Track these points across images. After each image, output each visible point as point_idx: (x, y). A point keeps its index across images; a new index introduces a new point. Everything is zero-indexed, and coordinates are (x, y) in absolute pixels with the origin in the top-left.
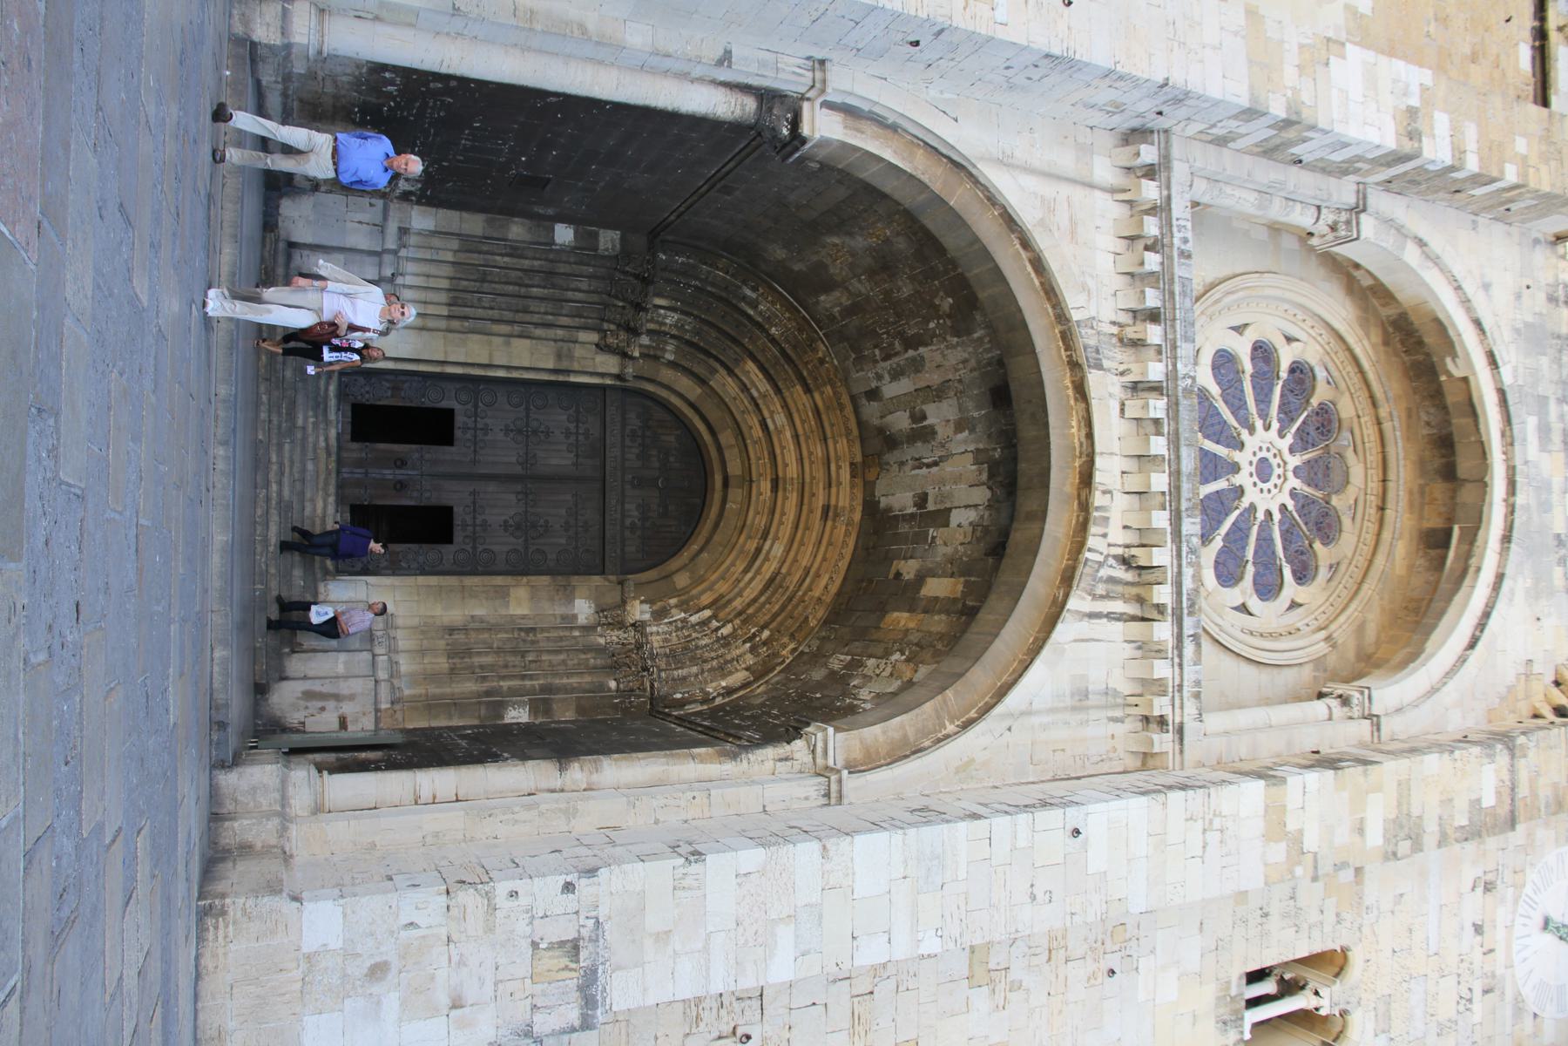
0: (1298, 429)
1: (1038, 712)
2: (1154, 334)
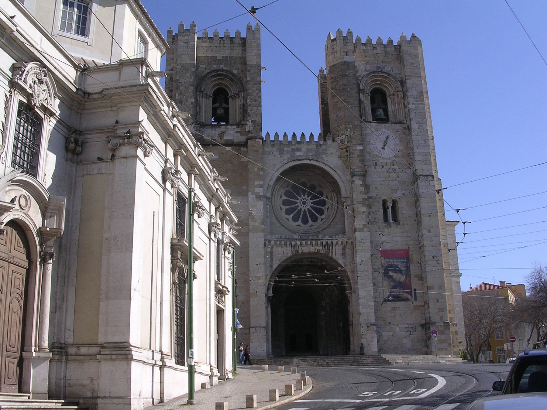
1: (345, 261)
2: (293, 243)
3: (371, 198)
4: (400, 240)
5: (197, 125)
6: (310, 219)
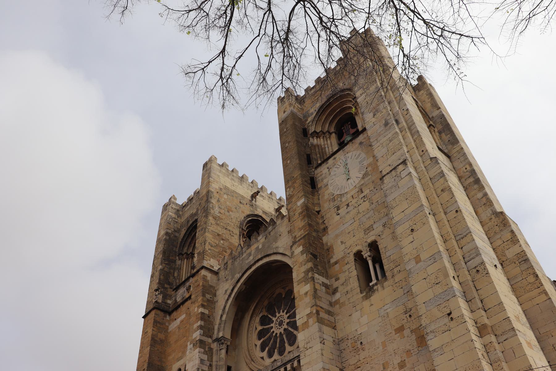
0: (272, 316)
3: (336, 263)
4: (391, 309)
5: (174, 290)
6: (286, 345)
